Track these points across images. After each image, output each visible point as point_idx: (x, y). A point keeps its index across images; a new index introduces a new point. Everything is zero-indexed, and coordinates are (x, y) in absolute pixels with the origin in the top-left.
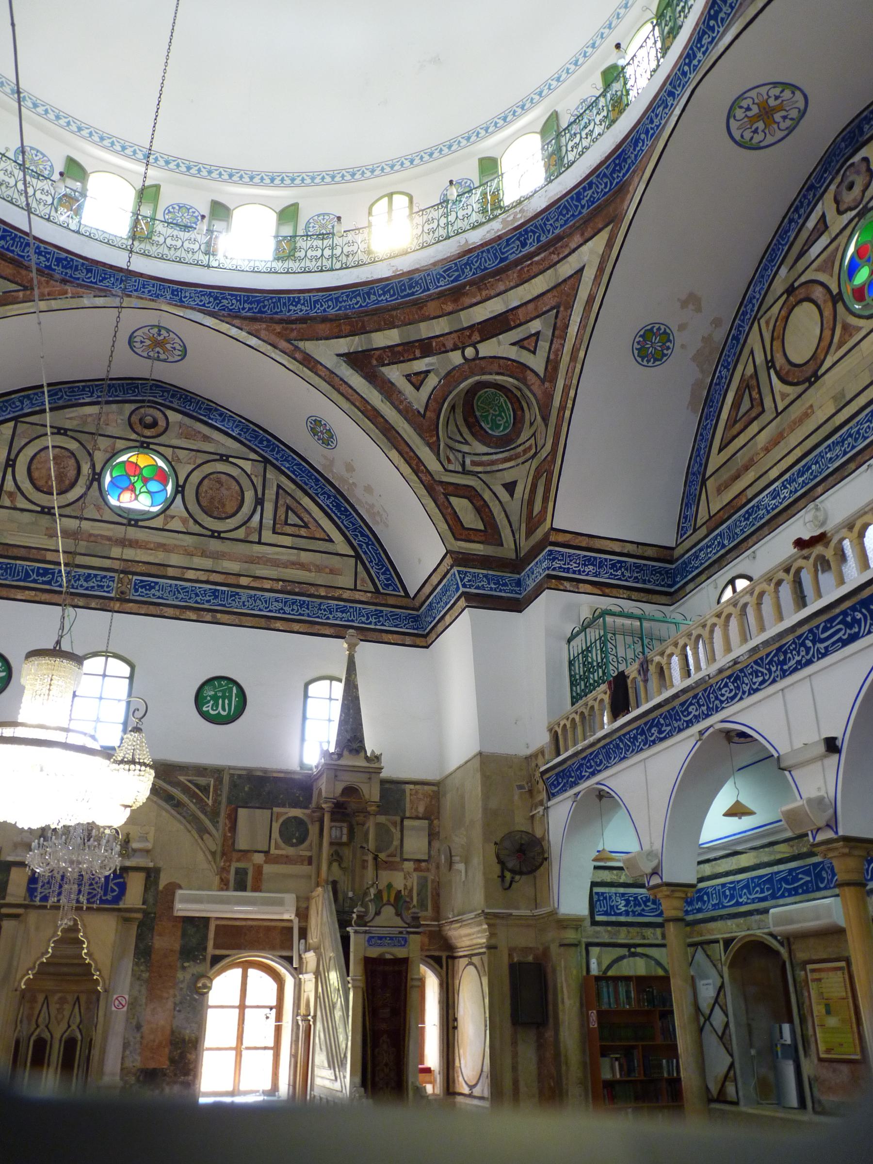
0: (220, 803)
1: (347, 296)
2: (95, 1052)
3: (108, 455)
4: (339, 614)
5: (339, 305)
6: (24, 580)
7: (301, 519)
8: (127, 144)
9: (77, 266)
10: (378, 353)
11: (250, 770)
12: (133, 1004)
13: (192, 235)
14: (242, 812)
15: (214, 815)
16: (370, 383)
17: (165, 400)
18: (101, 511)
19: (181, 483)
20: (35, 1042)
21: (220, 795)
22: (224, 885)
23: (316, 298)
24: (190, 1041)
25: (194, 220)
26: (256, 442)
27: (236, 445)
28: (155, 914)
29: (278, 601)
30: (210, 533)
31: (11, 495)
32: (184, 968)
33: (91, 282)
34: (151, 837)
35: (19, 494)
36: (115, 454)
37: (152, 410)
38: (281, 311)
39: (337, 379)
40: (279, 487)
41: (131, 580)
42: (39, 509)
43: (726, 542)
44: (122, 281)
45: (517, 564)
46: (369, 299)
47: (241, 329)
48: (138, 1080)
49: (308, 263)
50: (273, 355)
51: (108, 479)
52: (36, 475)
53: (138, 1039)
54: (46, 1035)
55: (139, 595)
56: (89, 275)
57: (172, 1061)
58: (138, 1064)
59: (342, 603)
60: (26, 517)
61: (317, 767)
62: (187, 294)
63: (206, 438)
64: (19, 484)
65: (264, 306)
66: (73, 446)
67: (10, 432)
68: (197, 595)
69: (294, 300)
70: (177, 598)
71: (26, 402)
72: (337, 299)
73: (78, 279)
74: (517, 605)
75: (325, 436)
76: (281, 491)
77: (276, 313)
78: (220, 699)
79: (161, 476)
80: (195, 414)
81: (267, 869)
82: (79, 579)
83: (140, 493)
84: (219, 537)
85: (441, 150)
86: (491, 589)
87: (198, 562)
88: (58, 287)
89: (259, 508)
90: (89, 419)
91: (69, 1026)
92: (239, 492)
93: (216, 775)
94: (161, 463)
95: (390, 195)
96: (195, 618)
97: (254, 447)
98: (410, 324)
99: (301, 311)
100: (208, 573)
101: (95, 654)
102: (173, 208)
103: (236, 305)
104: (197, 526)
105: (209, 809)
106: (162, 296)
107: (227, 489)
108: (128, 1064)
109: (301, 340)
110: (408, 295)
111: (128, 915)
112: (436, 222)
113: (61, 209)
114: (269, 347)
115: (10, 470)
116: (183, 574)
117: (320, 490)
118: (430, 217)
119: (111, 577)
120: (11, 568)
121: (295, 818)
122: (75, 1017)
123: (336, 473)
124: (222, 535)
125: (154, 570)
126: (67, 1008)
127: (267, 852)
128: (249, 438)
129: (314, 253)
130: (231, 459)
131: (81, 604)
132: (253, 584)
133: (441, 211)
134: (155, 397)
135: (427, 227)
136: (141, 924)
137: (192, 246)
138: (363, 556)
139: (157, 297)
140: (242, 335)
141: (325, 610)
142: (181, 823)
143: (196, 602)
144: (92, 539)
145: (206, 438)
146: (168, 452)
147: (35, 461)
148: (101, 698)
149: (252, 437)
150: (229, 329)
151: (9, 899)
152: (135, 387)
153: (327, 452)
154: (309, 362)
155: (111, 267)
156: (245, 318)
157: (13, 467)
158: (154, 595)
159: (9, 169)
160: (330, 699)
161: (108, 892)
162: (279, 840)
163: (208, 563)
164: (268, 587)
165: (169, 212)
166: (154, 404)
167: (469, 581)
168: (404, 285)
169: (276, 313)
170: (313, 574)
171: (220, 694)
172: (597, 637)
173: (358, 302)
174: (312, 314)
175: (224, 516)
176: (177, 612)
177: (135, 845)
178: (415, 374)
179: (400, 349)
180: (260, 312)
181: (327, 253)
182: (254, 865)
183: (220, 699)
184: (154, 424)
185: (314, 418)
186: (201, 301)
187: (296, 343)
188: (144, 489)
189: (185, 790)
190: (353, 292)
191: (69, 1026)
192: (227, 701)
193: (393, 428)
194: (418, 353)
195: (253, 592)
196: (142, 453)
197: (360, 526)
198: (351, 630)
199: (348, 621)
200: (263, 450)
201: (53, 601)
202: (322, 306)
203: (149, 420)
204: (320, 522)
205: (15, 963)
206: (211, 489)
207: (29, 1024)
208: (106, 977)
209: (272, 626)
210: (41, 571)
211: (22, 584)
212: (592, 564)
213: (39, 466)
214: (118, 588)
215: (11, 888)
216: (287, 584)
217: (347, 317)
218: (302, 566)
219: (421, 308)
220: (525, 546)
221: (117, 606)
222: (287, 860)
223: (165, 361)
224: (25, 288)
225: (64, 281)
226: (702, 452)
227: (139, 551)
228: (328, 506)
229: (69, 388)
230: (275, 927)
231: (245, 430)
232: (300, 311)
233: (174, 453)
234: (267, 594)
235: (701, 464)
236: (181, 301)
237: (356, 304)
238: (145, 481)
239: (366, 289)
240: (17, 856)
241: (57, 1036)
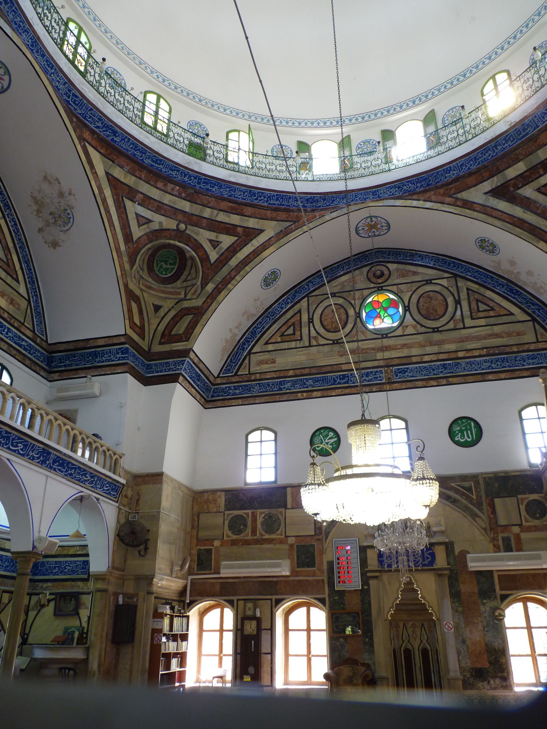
0: (481, 497)
1: (482, 154)
2: (441, 657)
3: (361, 301)
4: (531, 361)
5: (478, 161)
6: (334, 384)
7: (488, 306)
8: (326, 120)
9: (317, 199)
10: (512, 182)
11: (495, 473)
12: (457, 627)
13: (376, 155)
14: (497, 501)
15: (479, 505)
16: (512, 203)
17: (384, 258)
18: (365, 334)
19: (407, 304)
20: (404, 651)
21: (480, 492)
22: (497, 549)
23: (461, 163)
24: (499, 650)
25: (374, 146)
26: (446, 266)
27: (434, 272)
28: (457, 570)
29: (486, 362)
30: (432, 330)
31: (315, 338)
32: (484, 604)
33: (327, 205)
34: (443, 522)
35: (319, 337)
36: (364, 299)
37: (378, 267)
38: (441, 180)
39: (488, 209)
40: (468, 289)
41: (392, 370)
42: (332, 342)
44: (343, 198)
46: (497, 150)
47: (419, 200)
48: (472, 675)
49: (450, 143)
50: (443, 209)
51: (364, 314)
52: (325, 323)
53: (465, 649)
54: (410, 647)
55: (399, 378)
56: (325, 202)
57: (490, 663)
58: (469, 665)
59: (531, 353)
60: (326, 348)
61: (541, 464)
62: (382, 191)
63: (415, 273)
64: (318, 331)
65: (430, 181)
66: (341, 301)
67: (306, 304)
68: (434, 370)
69: (447, 170)
70: (422, 374)
71: (310, 285)
72: (475, 158)
73: (320, 206)
75: (490, 248)
76: (470, 292)
77: (438, 182)
78: (466, 431)
79: (394, 304)
80: (404, 261)
81: (524, 536)
83: (384, 317)
84: (438, 331)
85: (521, 31)
87: (429, 349)
88: (311, 215)
89: (459, 306)
90: (345, 284)
91: (422, 642)
92: (444, 300)
93: (474, 480)
94: (392, 296)
95: (493, 77)
96: (436, 384)
97: (446, 269)
98: (531, 154)
99: (454, 174)
100: (437, 355)
101: (383, 418)
102: (361, 145)
103: (412, 187)
104: (423, 328)
105: (475, 502)
106: (367, 198)
107: (436, 300)
108: (463, 665)
109: (459, 193)
110: (524, 136)
111: (440, 572)
112: (531, 80)
113: (302, 172)
114: (439, 205)
115: (311, 324)
116: (422, 359)
117: (495, 284)
118: (526, 78)
119: (380, 371)
120: (325, 379)
121: (534, 500)
122: (423, 636)
123: (504, 269)
124: (440, 329)
125: (404, 361)
126: (418, 630)
127: (520, 525)
128: (441, 265)
129: (453, 136)
130: (433, 281)
131: (367, 390)
132: (467, 355)
133: (533, 71)
134: (379, 258)
135: (525, 86)
136: (450, 578)
137: (377, 162)
138: (538, 318)
139: (365, 200)
140: (420, 203)
141: (520, 360)
142: (459, 512)
143: (434, 374)
144: (364, 351)
145: (415, 273)
146: (394, 288)
147: (323, 316)
148: (392, 443)
149: (442, 264)
150: (412, 203)
151: (370, 568)
152: (366, 257)
153: (494, 258)
154: (467, 205)
155: (335, 193)
156: (420, 193)
157: (313, 322)
158: (408, 376)
159: (271, 161)
160: (539, 418)
161: (425, 559)
162: (527, 516)
163: (435, 349)
164: (477, 354)
165: (359, 148)
166: (379, 263)
168: (519, 130)
169: (438, 182)
170: (505, 339)
171: (464, 428)
173: (490, 154)
174: (461, 174)
175: (437, 317)
176: (424, 383)
177: (434, 529)
178: (543, 186)
179: (528, 173)
180: (428, 185)
181: (461, 131)
182: (514, 534)
183: (466, 431)
184: (382, 274)
185: (480, 239)
186: (391, 192)
187: (455, 196)
188: (386, 314)
189: (457, 491)
190: (484, 150)
191: (422, 642)
192: (469, 432)
193: (537, 227)
194: (541, 172)
195: (468, 360)
196: (380, 294)
197: (530, 299)
198: (542, 370)
199: (538, 364)
200: (452, 269)
201: (352, 392)
202: (466, 166)
203: (378, 273)
204: (501, 304)
205: (382, 605)
206: (425, 303)
207: (398, 639)
208: (437, 611)
209: (486, 379)
210: (341, 377)
211: (333, 386)
213: (326, 318)
214: (386, 376)
215: (369, 561)
216: (489, 349)
217: (485, 167)
218: (497, 336)
219: (536, 141)
221: (388, 387)
222: (536, 529)
223: (379, 235)
224: (295, 222)
225: (313, 211)
227: (392, 352)
228: (504, 292)
229: (330, 269)
230: (538, 574)
231: (437, 261)
232: (453, 175)
233: (398, 288)
234: (477, 359)
236: (379, 197)
237: (489, 156)
238: (385, 309)
239: (493, 144)
240: (368, 542)
241: (416, 648)
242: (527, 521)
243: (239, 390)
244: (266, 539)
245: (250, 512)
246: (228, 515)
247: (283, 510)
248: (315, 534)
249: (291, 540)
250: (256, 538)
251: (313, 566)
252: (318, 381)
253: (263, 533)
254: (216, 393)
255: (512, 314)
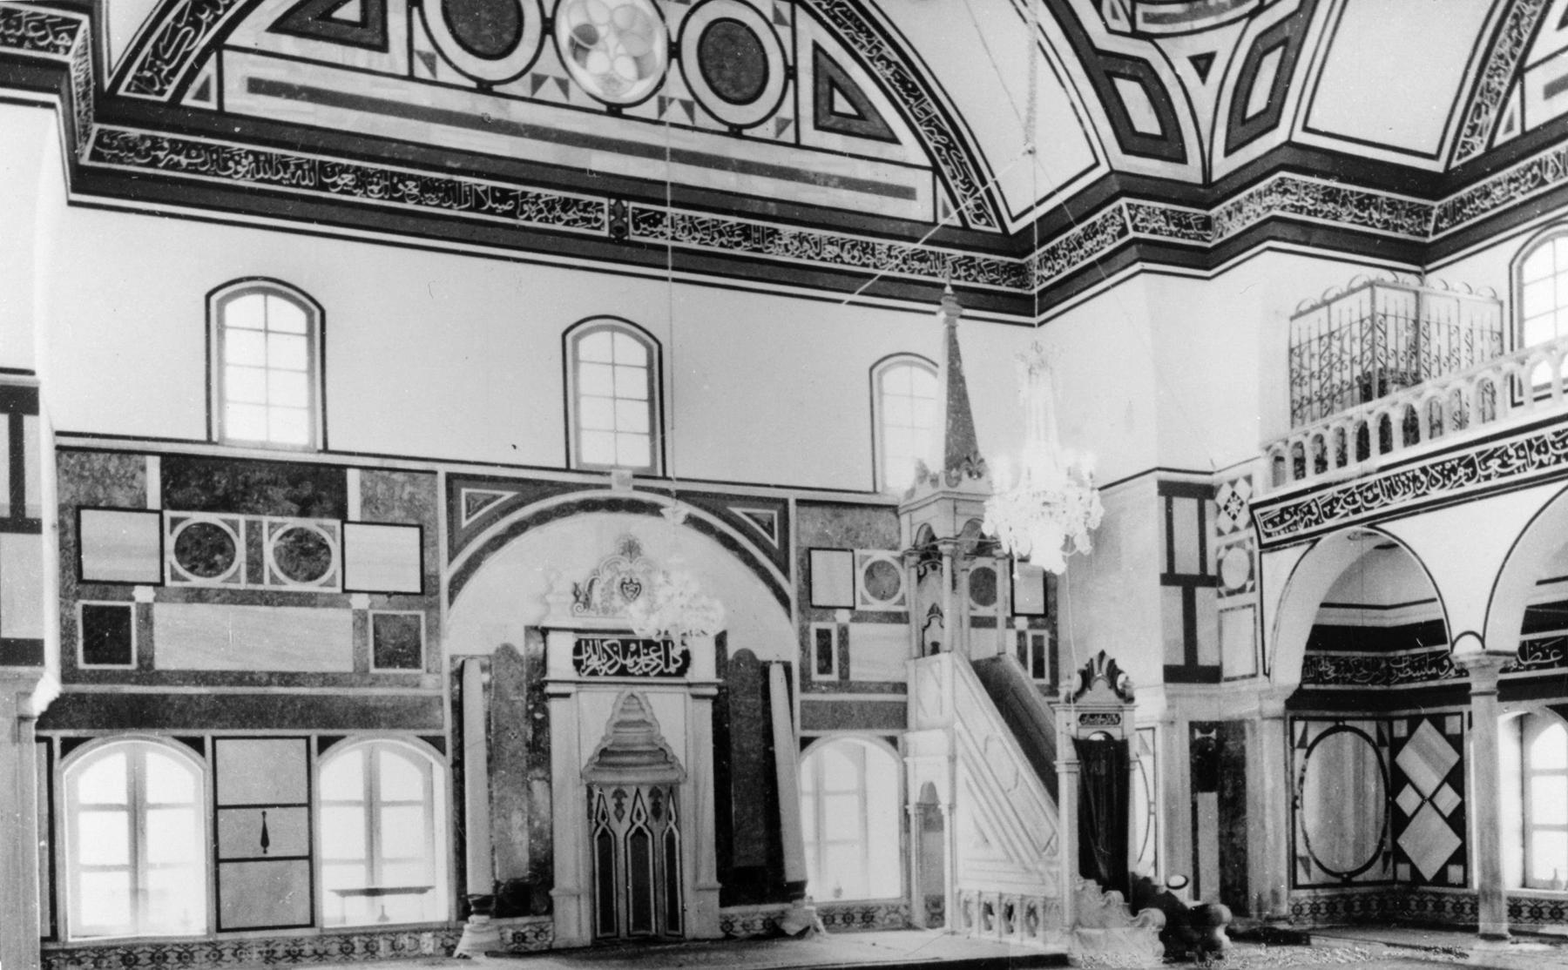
41: (625, 210)
43: (1549, 176)
45: (1210, 192)
74: (1206, 259)
82: (553, 208)
86: (1171, 234)
89: (791, 83)
143: (722, 245)
167: (1143, 220)
172: (1356, 318)
212: (1336, 202)
214: (611, 223)
220: (1223, 166)
226: (1524, 21)
235: (1518, 43)
242: (865, 602)
243: (188, 156)
244: (289, 593)
245: (242, 519)
246: (175, 522)
247: (337, 523)
248: (422, 593)
249: (360, 602)
250: (259, 587)
251: (416, 665)
252: (438, 189)
253: (281, 576)
254: (109, 146)
255: (894, 140)
